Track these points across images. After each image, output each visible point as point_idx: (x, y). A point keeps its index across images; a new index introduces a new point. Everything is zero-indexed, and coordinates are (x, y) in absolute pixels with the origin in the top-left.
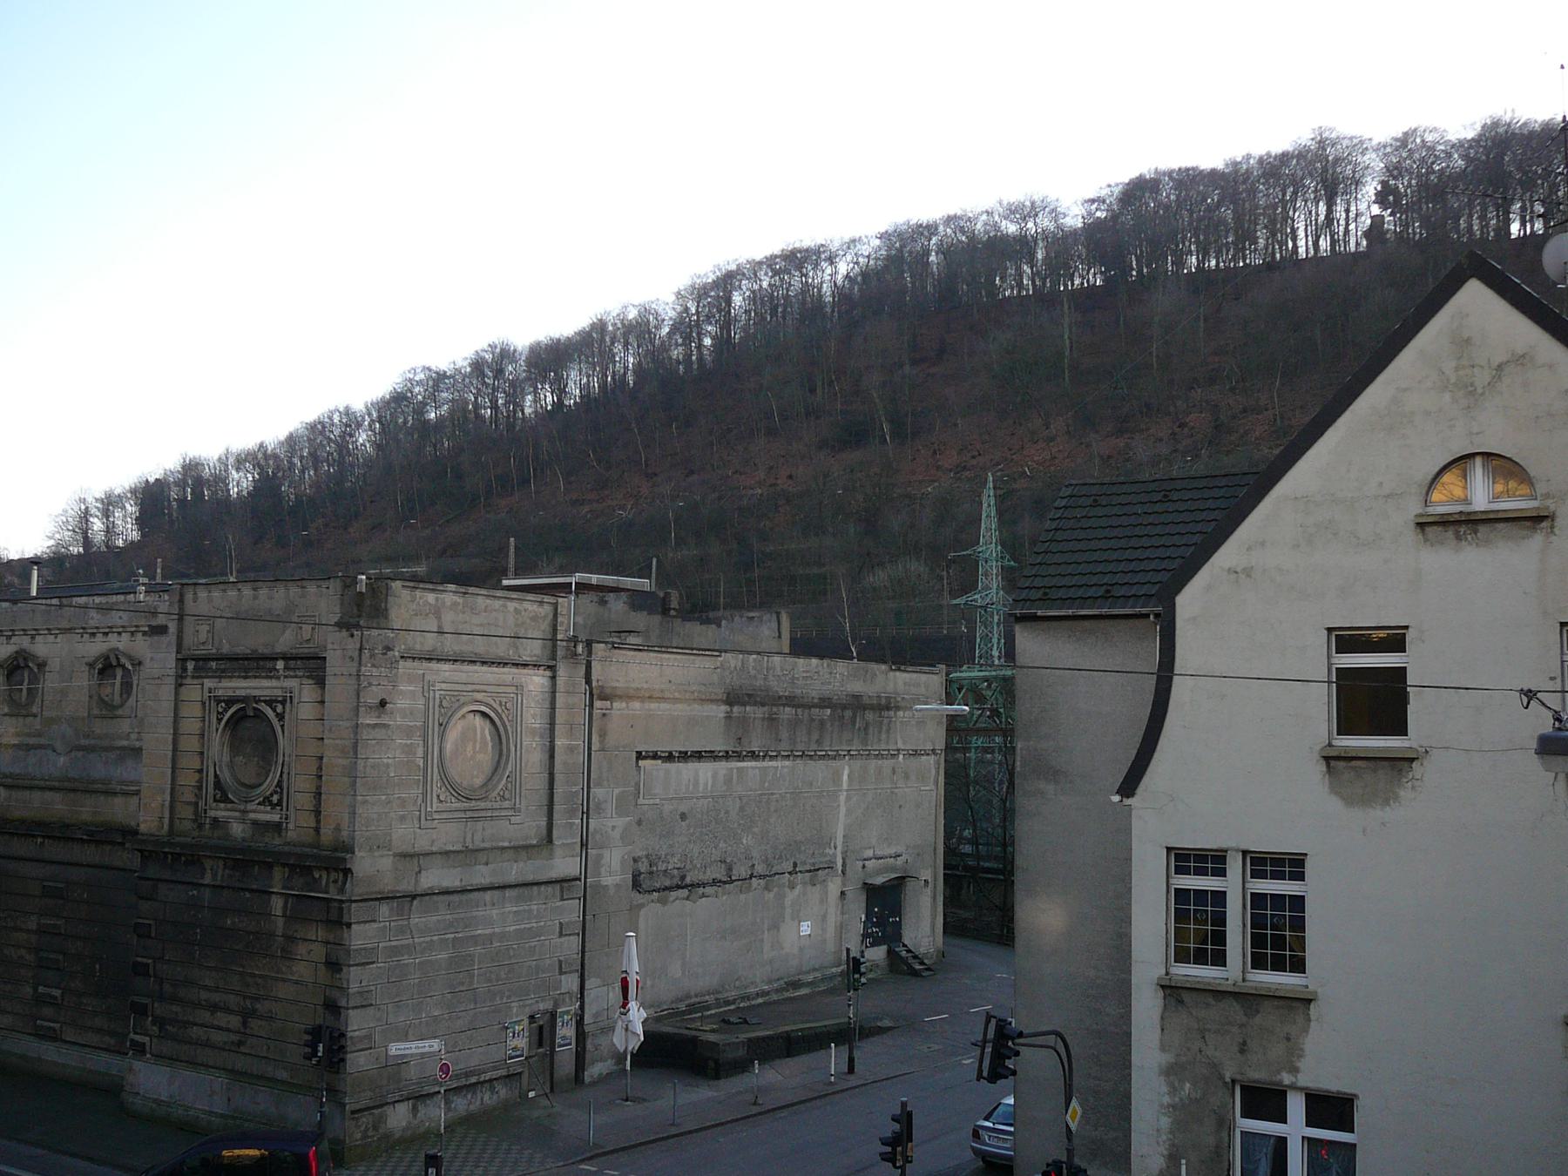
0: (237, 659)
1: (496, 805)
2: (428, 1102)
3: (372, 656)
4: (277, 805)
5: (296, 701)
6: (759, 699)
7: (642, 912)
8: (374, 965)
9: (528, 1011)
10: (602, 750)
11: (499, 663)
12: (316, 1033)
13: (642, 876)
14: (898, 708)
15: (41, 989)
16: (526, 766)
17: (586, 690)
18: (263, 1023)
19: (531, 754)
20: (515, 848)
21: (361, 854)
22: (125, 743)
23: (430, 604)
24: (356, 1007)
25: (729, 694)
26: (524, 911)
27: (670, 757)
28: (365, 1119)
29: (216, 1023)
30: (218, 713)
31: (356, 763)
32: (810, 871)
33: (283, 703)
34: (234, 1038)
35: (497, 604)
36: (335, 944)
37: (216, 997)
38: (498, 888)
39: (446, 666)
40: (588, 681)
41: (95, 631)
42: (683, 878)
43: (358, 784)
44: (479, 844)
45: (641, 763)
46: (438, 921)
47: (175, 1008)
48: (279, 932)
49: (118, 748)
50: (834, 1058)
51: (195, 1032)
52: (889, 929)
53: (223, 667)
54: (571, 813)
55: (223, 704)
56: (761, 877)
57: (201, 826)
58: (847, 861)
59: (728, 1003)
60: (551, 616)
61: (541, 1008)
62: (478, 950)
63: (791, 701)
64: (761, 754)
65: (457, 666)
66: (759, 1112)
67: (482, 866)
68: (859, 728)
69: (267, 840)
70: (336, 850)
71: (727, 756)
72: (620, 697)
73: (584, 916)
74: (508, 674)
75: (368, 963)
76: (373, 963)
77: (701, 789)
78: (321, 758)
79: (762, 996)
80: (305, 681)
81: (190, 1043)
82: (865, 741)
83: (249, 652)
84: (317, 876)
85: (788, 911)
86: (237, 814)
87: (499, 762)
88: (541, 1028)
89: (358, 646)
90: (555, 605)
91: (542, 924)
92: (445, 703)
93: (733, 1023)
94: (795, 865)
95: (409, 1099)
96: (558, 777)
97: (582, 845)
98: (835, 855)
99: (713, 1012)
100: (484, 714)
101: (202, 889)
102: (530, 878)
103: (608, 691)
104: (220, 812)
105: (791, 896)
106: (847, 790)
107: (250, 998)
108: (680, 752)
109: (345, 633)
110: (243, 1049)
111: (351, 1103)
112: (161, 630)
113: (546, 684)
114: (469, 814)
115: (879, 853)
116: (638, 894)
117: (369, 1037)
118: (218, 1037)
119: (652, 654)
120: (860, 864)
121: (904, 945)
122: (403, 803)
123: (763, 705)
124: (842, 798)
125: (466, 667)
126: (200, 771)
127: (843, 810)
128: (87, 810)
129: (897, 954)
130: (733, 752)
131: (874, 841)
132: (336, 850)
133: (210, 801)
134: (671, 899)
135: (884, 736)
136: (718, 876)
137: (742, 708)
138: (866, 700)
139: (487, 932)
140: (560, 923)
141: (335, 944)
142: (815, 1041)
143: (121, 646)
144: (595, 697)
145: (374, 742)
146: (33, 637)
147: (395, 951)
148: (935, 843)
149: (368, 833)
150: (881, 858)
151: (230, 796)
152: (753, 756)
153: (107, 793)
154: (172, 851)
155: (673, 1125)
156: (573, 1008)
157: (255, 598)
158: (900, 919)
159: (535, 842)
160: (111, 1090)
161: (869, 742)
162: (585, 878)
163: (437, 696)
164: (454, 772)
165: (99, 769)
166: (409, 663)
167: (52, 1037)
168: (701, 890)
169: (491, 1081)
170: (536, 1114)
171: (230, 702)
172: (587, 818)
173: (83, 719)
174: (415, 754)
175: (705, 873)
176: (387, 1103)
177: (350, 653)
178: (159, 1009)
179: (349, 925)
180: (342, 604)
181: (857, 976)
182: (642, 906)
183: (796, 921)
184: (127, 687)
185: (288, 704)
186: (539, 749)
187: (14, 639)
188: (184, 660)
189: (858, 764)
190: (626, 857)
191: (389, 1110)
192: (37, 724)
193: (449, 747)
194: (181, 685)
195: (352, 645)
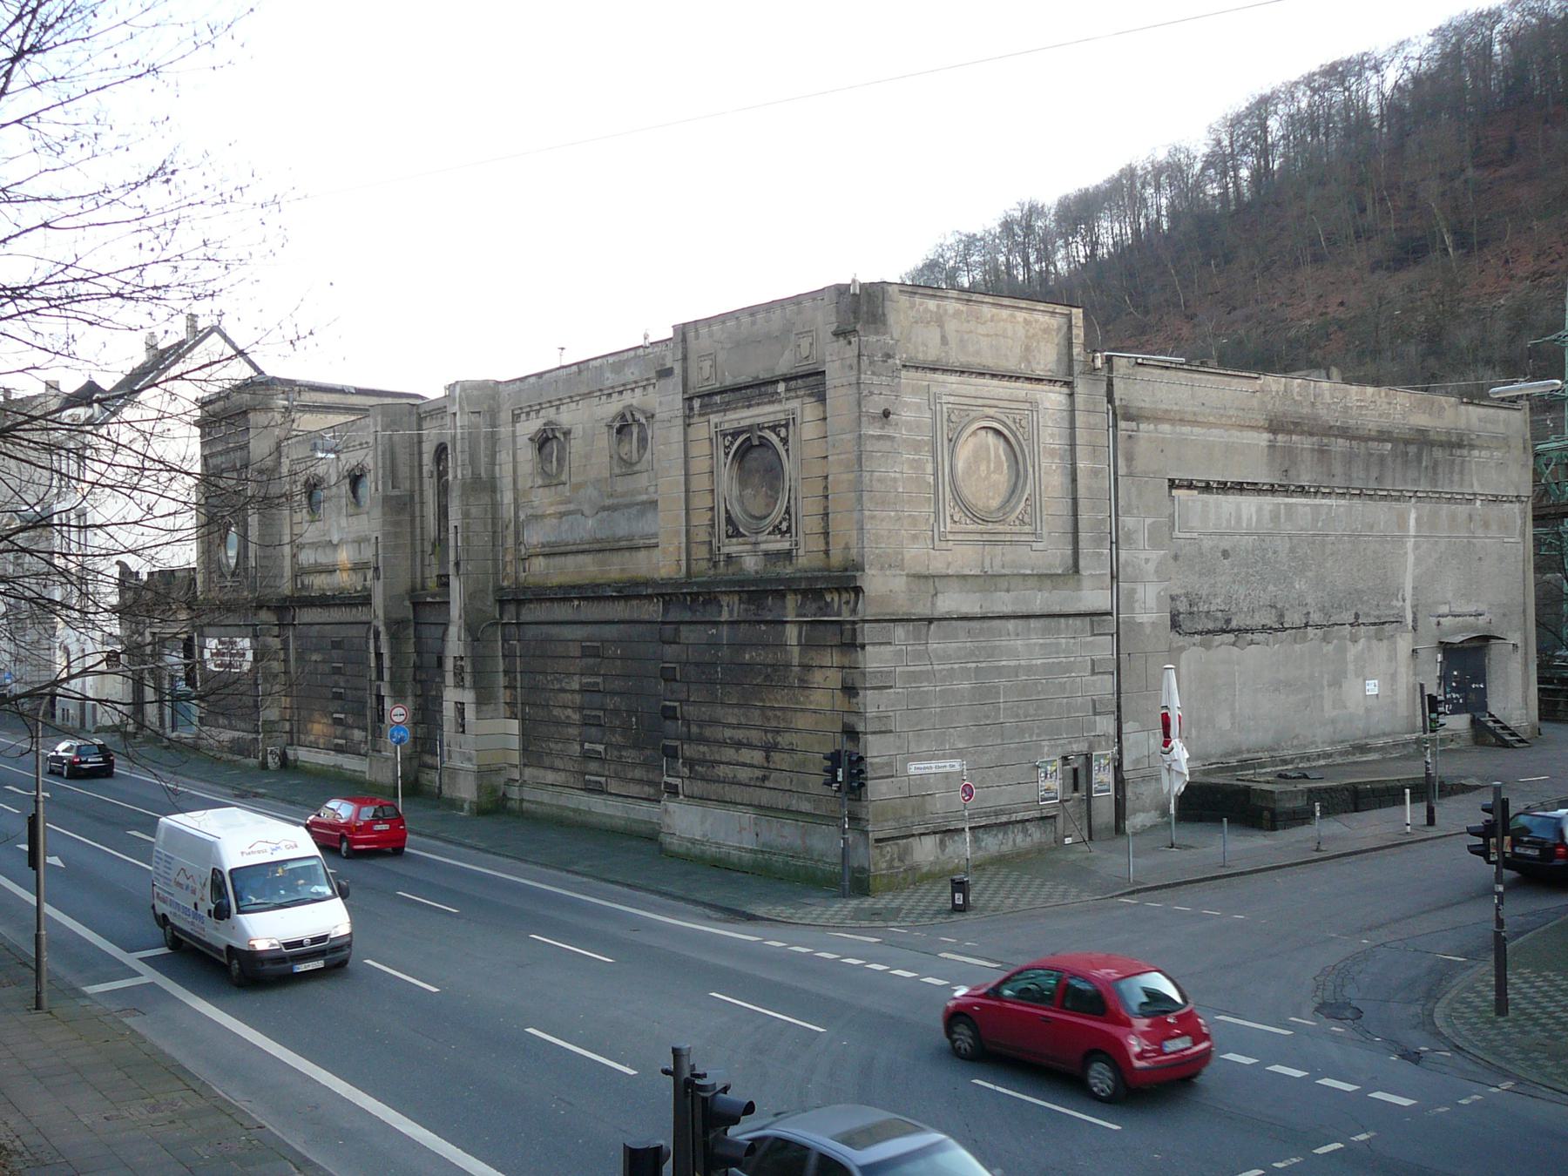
0: (740, 389)
1: (1015, 529)
2: (956, 838)
3: (872, 363)
4: (786, 532)
5: (798, 421)
6: (1306, 429)
7: (1184, 655)
8: (892, 690)
9: (1060, 752)
10: (1130, 475)
11: (1011, 377)
12: (835, 758)
13: (1181, 616)
14: (1472, 447)
15: (587, 746)
16: (1046, 487)
17: (1108, 409)
18: (785, 756)
19: (1050, 477)
20: (1040, 576)
21: (873, 572)
22: (644, 497)
23: (931, 312)
24: (874, 733)
25: (1271, 421)
26: (1050, 644)
27: (1207, 488)
28: (889, 848)
29: (741, 760)
30: (726, 447)
31: (861, 476)
32: (1374, 624)
33: (786, 426)
34: (759, 773)
35: (1005, 313)
36: (850, 668)
37: (740, 734)
38: (1022, 617)
39: (953, 378)
40: (1110, 400)
41: (611, 391)
42: (1228, 621)
43: (864, 498)
44: (997, 570)
45: (1174, 492)
46: (959, 648)
47: (702, 749)
48: (796, 661)
49: (638, 504)
50: (1411, 813)
51: (722, 771)
52: (1472, 697)
53: (727, 400)
54: (1098, 542)
55: (730, 438)
56: (1317, 626)
57: (715, 565)
58: (1419, 616)
59: (1285, 762)
60: (1065, 329)
61: (1075, 750)
62: (1002, 682)
63: (1344, 432)
64: (1312, 490)
65: (965, 378)
66: (1319, 858)
67: (1003, 593)
68: (1426, 467)
69: (778, 570)
70: (846, 570)
71: (1272, 490)
72: (1148, 418)
73: (1118, 654)
74: (1021, 389)
75: (886, 688)
76: (891, 687)
77: (1244, 525)
78: (826, 477)
79: (1324, 758)
80: (807, 400)
81: (719, 782)
82: (1434, 482)
83: (750, 379)
84: (829, 600)
85: (1351, 667)
86: (748, 547)
87: (1016, 484)
88: (1075, 771)
89: (857, 352)
90: (1069, 317)
91: (1072, 659)
92: (953, 418)
93: (1291, 778)
94: (1357, 616)
95: (935, 833)
96: (1082, 503)
97: (1112, 577)
98: (1403, 609)
99: (1268, 770)
100: (998, 432)
101: (720, 627)
102: (1056, 609)
103: (1133, 411)
104: (733, 547)
105: (1353, 651)
106: (1415, 537)
107: (772, 731)
108: (1219, 482)
109: (842, 342)
110: (767, 784)
111: (875, 831)
112: (665, 373)
113: (1064, 402)
114: (986, 537)
115: (1457, 610)
116: (1177, 635)
117: (890, 764)
118: (744, 774)
119: (1181, 374)
120: (1434, 620)
121: (1491, 715)
122: (914, 520)
123: (1311, 434)
124: (1410, 543)
125: (974, 380)
126: (712, 509)
127: (1411, 558)
128: (615, 569)
129: (1484, 724)
130: (1280, 486)
131: (1449, 596)
132: (846, 570)
133: (723, 535)
134: (1216, 644)
135: (1456, 477)
136: (1269, 623)
137: (1287, 438)
138: (1433, 436)
139: (1012, 663)
140: (1092, 660)
141: (850, 668)
142: (1388, 796)
143: (635, 402)
144: (1119, 417)
145: (879, 454)
146: (558, 409)
147: (913, 677)
148: (1525, 603)
149: (877, 551)
150: (1459, 616)
151: (741, 530)
152: (1302, 491)
153: (630, 549)
154: (689, 590)
155: (1223, 866)
156: (1110, 752)
157: (754, 323)
158: (1485, 685)
159: (1060, 572)
160: (649, 838)
161: (1440, 483)
162: (1118, 614)
163: (945, 410)
164: (967, 492)
165: (623, 526)
166: (912, 374)
167: (599, 790)
168: (1249, 636)
169: (1023, 821)
170: (1072, 857)
171: (735, 434)
172: (1117, 549)
173: (606, 479)
174: (924, 470)
175: (1252, 617)
176: (913, 835)
177: (848, 362)
178: (689, 750)
179: (863, 647)
180: (838, 312)
181: (1434, 716)
182: (1182, 649)
183: (1361, 679)
184: (643, 441)
185: (791, 427)
186: (1059, 471)
187: (542, 413)
188: (690, 399)
189: (1427, 507)
190: (1162, 593)
191: (914, 841)
192: (566, 490)
193: (960, 465)
194: (689, 425)
195: (851, 352)
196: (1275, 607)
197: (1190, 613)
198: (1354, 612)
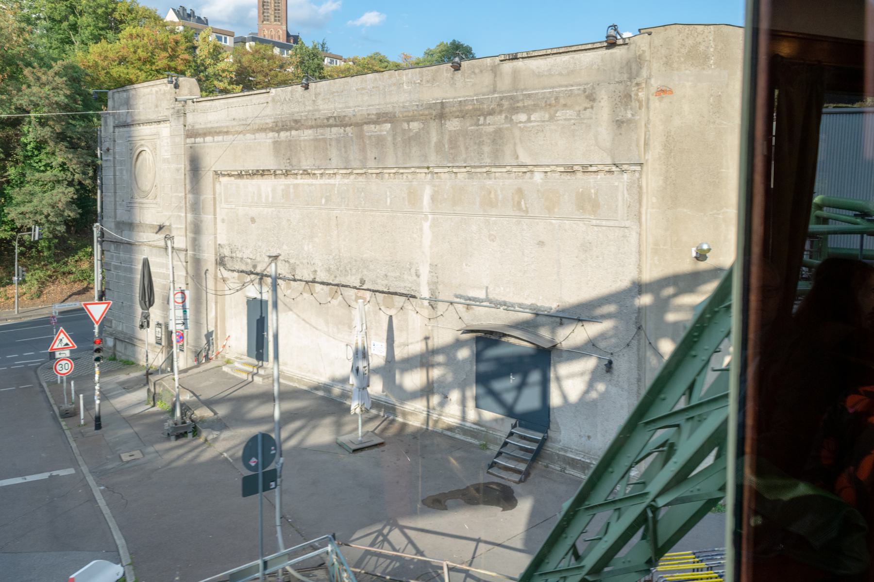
13: (226, 258)
27: (240, 175)
42: (255, 267)
77: (263, 200)
94: (363, 282)
137: (288, 133)
196: (288, 262)
197: (232, 257)
198: (359, 276)
